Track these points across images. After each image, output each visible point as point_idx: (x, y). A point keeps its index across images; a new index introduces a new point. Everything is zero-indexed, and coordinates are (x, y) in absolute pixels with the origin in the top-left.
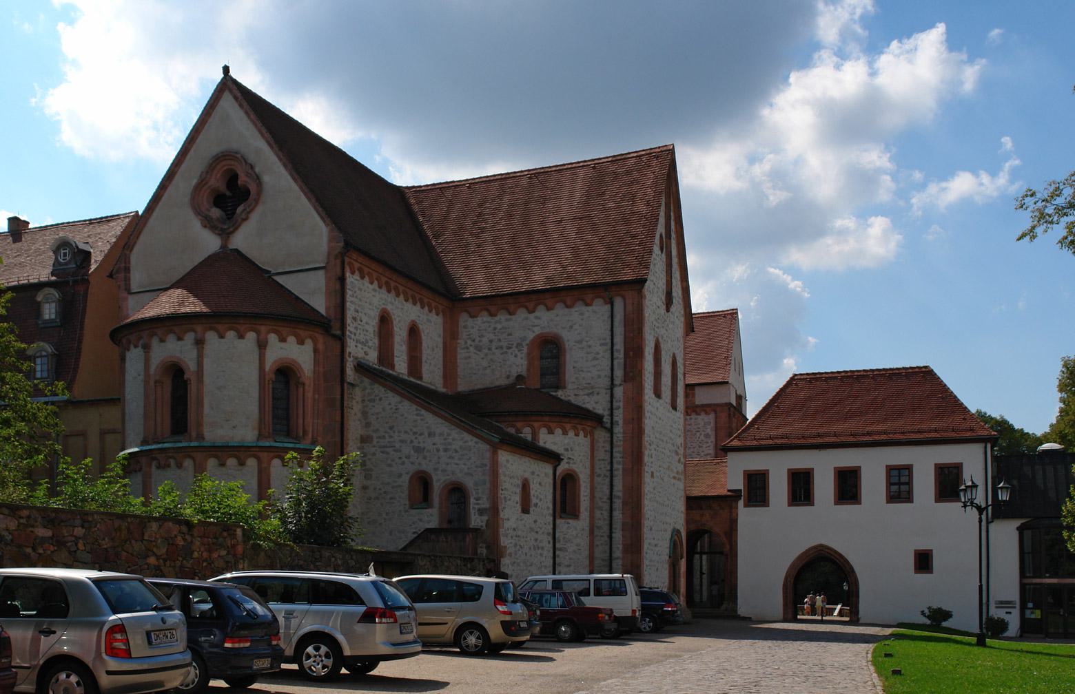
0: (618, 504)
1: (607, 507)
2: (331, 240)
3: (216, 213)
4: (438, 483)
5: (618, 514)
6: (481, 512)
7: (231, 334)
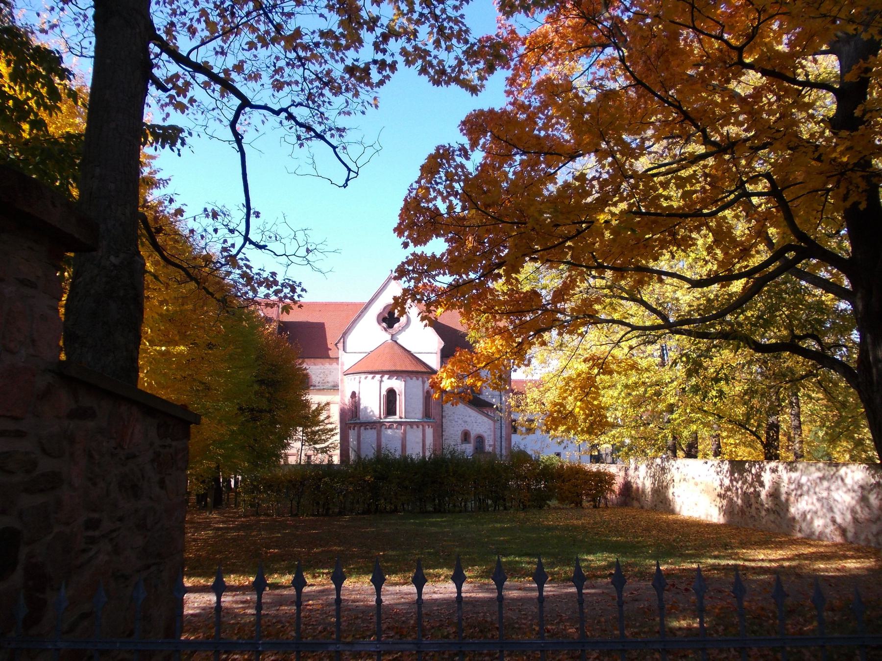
0: (503, 440)
1: (499, 440)
2: (439, 342)
3: (384, 325)
4: (473, 435)
5: (503, 443)
6: (490, 446)
7: (414, 378)
